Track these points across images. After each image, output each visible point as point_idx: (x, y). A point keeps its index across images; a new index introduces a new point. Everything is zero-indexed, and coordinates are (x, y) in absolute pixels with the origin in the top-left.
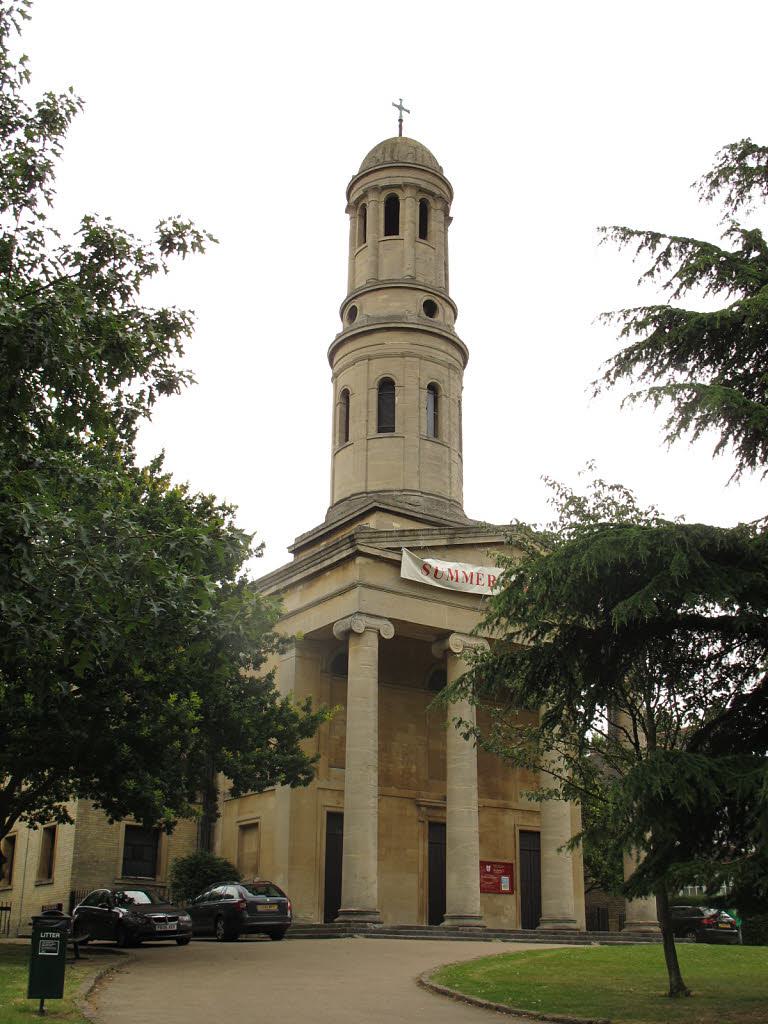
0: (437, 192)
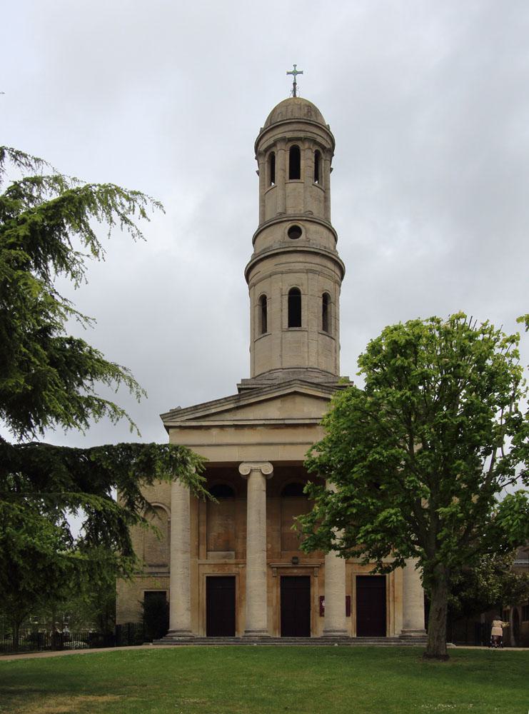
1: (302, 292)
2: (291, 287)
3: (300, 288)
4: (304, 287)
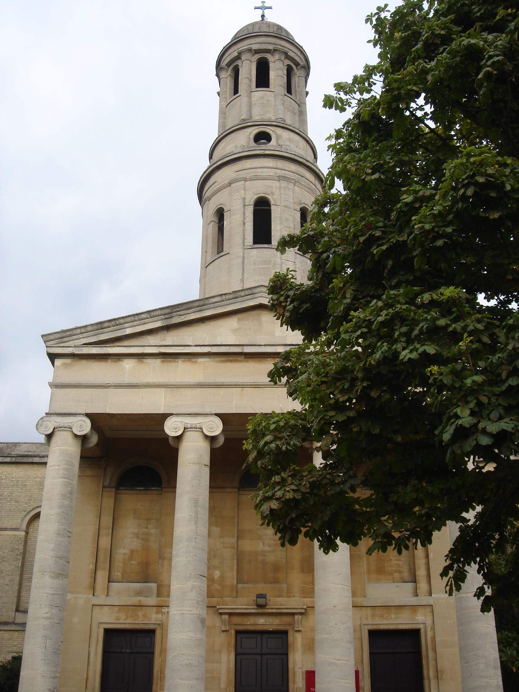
0: (271, 47)
1: (272, 202)
2: (257, 196)
3: (270, 197)
4: (275, 196)
